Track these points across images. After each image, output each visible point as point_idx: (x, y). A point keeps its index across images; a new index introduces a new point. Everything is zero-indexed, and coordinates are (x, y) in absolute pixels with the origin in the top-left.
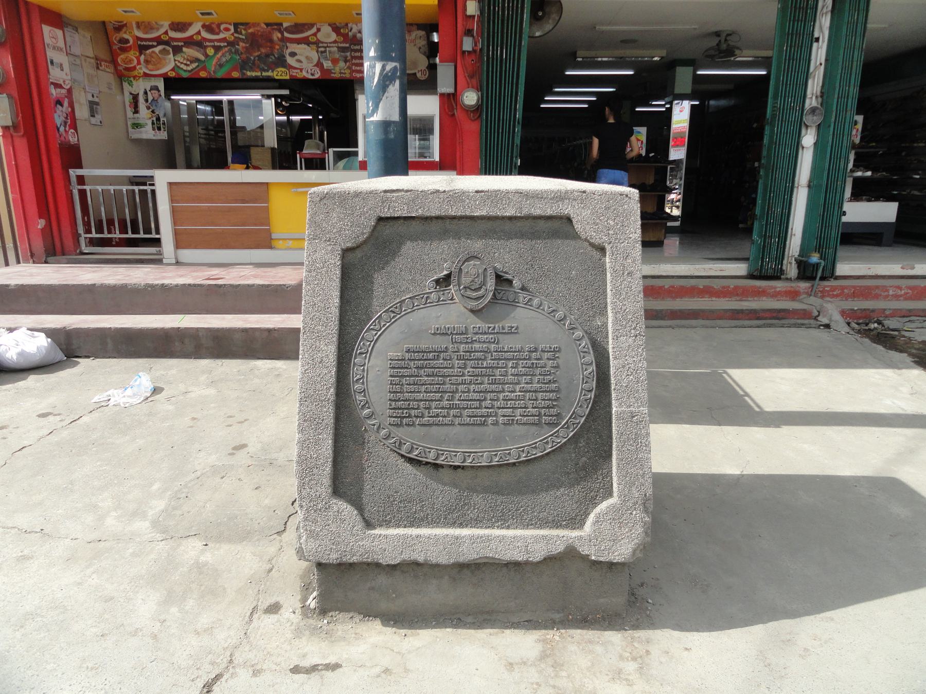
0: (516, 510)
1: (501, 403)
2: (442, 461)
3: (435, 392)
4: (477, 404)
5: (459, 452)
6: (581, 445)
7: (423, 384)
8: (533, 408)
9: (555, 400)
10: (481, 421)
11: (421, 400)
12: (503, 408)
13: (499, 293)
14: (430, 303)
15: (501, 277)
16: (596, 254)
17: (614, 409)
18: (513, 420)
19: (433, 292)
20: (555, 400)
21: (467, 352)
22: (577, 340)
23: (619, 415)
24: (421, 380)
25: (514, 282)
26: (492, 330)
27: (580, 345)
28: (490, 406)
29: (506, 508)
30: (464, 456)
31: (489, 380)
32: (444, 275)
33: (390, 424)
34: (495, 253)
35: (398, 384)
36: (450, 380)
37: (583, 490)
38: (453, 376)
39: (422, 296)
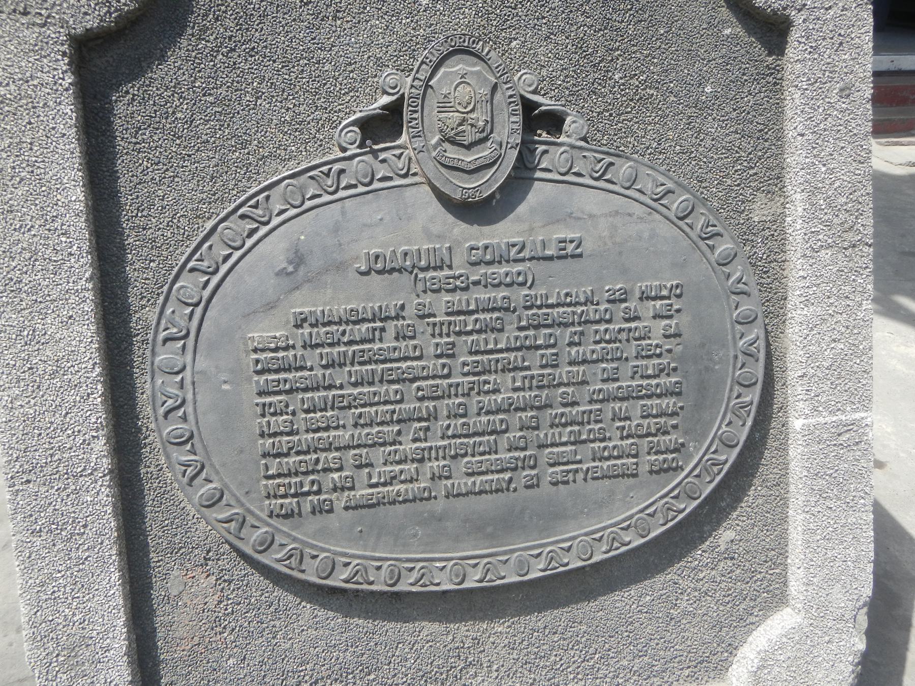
0: (582, 662)
1: (546, 435)
2: (411, 584)
3: (382, 423)
5: (451, 559)
6: (723, 504)
7: (349, 407)
8: (622, 438)
9: (674, 414)
11: (348, 447)
12: (553, 445)
14: (346, 188)
15: (537, 105)
17: (797, 424)
18: (576, 471)
20: (674, 414)
21: (459, 313)
22: (724, 265)
23: (809, 431)
24: (343, 396)
25: (569, 120)
26: (520, 252)
27: (728, 276)
28: (522, 444)
29: (561, 659)
31: (514, 380)
32: (384, 108)
33: (271, 516)
35: (281, 414)
36: (419, 389)
37: (727, 599)
38: (426, 378)
39: (325, 169)
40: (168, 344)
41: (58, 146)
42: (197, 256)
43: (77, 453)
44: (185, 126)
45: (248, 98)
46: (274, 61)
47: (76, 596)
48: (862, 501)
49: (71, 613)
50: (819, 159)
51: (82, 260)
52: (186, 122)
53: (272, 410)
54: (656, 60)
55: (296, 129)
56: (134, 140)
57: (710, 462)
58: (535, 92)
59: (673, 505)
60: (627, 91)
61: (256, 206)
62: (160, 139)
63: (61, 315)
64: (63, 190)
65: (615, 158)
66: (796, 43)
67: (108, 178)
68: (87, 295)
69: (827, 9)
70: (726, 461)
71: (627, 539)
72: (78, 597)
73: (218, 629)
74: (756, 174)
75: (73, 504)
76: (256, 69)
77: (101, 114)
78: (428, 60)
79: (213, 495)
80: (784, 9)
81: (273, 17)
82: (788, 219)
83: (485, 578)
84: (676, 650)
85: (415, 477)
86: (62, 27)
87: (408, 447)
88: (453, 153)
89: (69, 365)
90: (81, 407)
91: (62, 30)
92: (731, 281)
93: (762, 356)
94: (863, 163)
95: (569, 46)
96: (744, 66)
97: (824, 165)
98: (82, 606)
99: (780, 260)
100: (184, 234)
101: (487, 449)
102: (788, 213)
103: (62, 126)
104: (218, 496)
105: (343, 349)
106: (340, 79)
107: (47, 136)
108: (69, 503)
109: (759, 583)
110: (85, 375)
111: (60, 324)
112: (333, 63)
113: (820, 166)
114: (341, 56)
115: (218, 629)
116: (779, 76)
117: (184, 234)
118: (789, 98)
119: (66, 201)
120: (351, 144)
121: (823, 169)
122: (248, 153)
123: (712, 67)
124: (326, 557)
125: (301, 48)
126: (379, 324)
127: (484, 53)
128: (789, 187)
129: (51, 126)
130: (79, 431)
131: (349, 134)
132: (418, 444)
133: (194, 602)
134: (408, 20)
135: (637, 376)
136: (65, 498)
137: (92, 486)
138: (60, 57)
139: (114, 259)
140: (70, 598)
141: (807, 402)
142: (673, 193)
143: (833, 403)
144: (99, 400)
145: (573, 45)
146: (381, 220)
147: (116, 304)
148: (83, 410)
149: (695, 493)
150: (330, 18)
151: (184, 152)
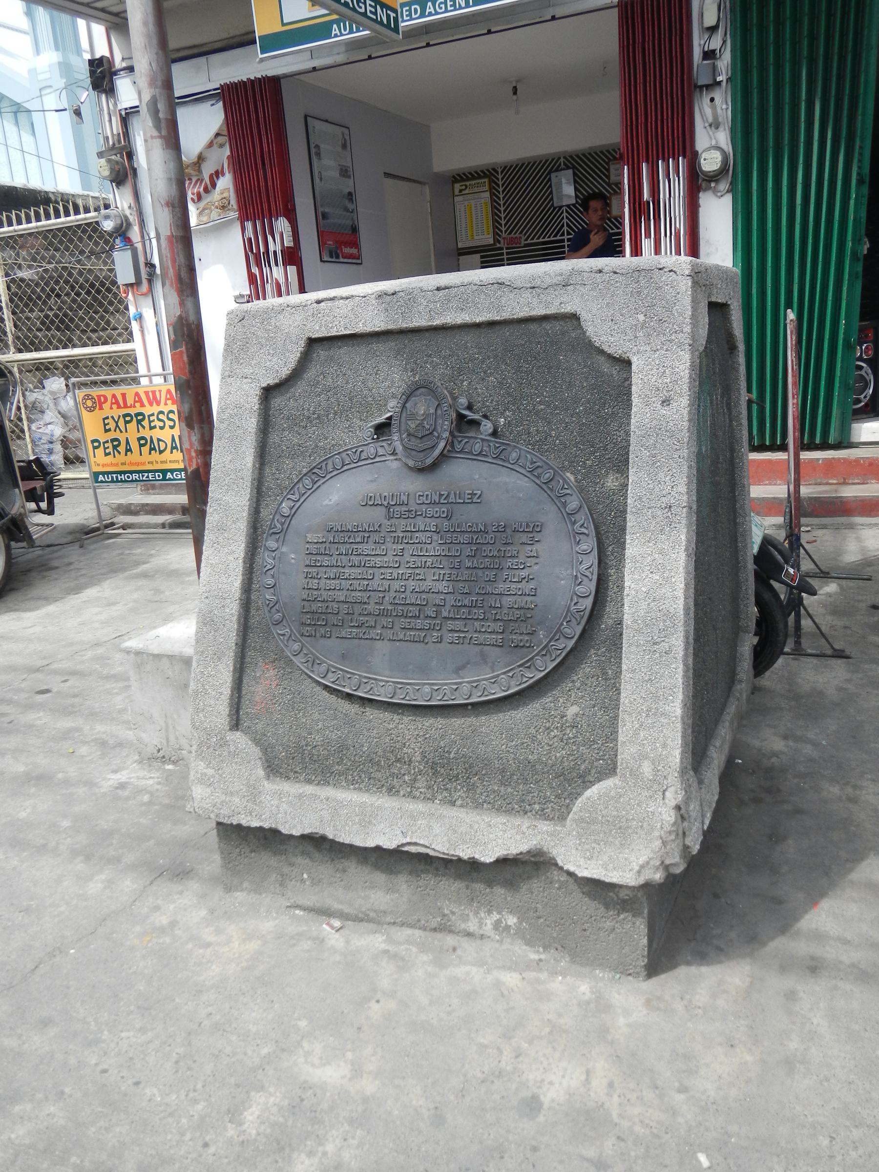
4: (414, 610)
5: (388, 682)
15: (464, 416)
30: (395, 688)
32: (387, 419)
34: (463, 381)
40: (273, 536)
42: (292, 492)
48: (671, 698)
61: (320, 469)
69: (655, 351)
73: (274, 701)
74: (609, 458)
80: (626, 353)
84: (530, 787)
88: (414, 442)
93: (595, 577)
94: (680, 450)
105: (348, 546)
109: (596, 752)
115: (274, 701)
126: (367, 535)
135: (508, 581)
142: (541, 467)
143: (649, 618)
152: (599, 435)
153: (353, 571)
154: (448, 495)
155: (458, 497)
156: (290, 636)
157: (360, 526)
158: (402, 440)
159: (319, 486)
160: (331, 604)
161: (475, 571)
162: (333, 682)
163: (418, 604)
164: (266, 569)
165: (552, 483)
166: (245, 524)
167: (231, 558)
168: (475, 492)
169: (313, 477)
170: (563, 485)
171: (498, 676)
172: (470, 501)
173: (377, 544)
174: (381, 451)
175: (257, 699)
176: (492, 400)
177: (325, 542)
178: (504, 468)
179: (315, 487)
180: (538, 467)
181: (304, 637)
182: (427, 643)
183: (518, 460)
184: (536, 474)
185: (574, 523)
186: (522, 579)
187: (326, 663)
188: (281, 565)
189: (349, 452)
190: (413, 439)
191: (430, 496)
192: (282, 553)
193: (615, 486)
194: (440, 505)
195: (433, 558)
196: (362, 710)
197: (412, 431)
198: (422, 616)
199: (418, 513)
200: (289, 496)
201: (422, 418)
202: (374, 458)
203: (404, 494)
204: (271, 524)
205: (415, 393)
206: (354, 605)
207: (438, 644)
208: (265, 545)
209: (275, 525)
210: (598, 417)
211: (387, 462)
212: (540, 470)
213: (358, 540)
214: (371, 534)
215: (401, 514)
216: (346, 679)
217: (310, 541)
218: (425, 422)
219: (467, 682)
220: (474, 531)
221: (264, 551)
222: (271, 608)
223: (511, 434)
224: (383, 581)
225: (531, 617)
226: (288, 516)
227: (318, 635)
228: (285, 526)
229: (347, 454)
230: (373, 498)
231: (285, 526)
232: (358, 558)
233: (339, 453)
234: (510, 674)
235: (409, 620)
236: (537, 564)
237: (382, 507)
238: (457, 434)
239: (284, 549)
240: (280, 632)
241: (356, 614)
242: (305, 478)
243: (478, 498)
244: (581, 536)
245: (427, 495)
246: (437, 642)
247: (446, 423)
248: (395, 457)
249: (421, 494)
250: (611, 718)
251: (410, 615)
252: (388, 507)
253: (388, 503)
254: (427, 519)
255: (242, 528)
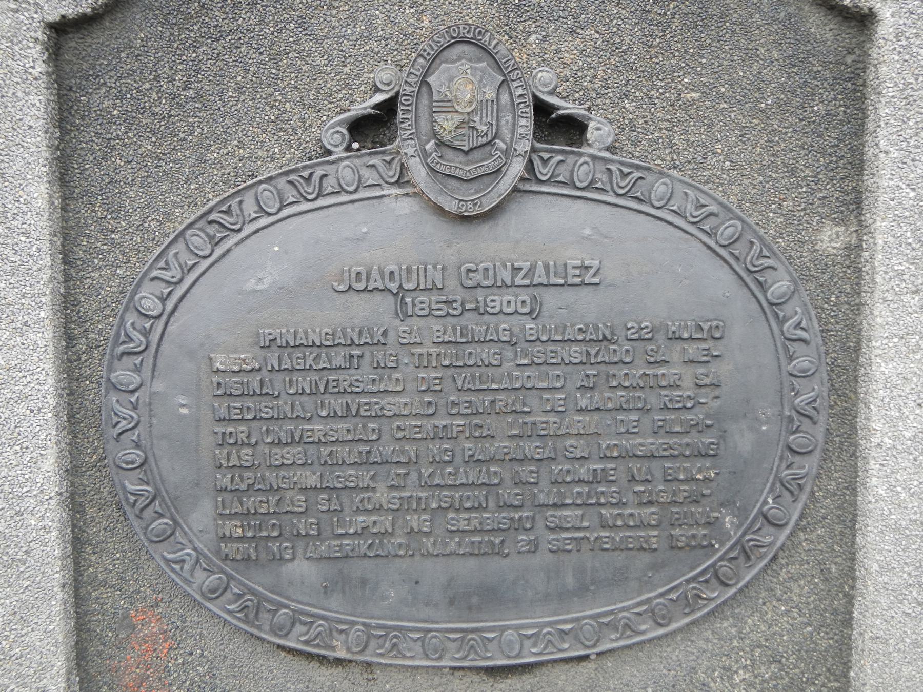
5: (430, 630)
8: (641, 504)
10: (492, 544)
13: (545, 162)
15: (552, 108)
16: (848, 35)
19: (340, 160)
25: (592, 125)
32: (377, 106)
34: (530, 34)
40: (125, 358)
41: (24, 139)
42: (162, 264)
43: (23, 472)
44: (163, 123)
45: (231, 94)
46: (261, 53)
47: (14, 627)
49: (8, 646)
50: (907, 182)
51: (41, 262)
52: (164, 117)
53: (232, 441)
54: (704, 61)
55: (281, 129)
56: (109, 136)
57: (752, 543)
58: (552, 92)
59: (702, 591)
60: (667, 95)
61: (228, 212)
62: (135, 136)
63: (16, 320)
64: (26, 186)
65: (646, 172)
66: (881, 41)
67: (78, 176)
68: (43, 300)
70: (771, 544)
71: (643, 627)
72: (16, 630)
75: (16, 526)
76: (241, 62)
77: (76, 107)
78: (426, 53)
79: (164, 531)
81: (262, 6)
82: (866, 254)
83: (466, 656)
85: (390, 531)
86: (36, 13)
87: (382, 495)
89: (21, 375)
90: (31, 422)
91: (35, 16)
92: (787, 325)
95: (599, 42)
96: (815, 69)
97: (914, 190)
98: (20, 640)
99: (852, 303)
100: (154, 239)
101: (476, 505)
102: (864, 246)
103: (29, 118)
104: (169, 532)
106: (333, 75)
107: (13, 128)
108: (12, 526)
110: (37, 387)
111: (14, 330)
112: (325, 57)
113: (908, 190)
114: (335, 49)
116: (860, 82)
117: (154, 239)
118: (870, 108)
119: (29, 198)
120: (336, 146)
121: (912, 194)
122: (227, 154)
123: (775, 69)
124: (284, 614)
125: (291, 39)
126: (356, 352)
127: (491, 47)
128: (868, 215)
129: (18, 117)
130: (27, 448)
131: (336, 136)
132: (395, 494)
133: (143, 648)
134: (412, 10)
135: (662, 431)
136: (8, 519)
137: (37, 509)
138: (31, 45)
139: (79, 263)
140: (7, 629)
141: (881, 480)
144: (50, 415)
145: (603, 41)
146: (365, 233)
147: (79, 311)
148: (32, 425)
149: (731, 579)
150: (325, 7)
151: (159, 151)
152: (803, 152)
153: (332, 426)
154: (532, 269)
155: (552, 275)
156: (197, 561)
157: (339, 334)
158: (425, 155)
159: (228, 251)
160: (288, 495)
161: (596, 416)
162: (306, 643)
163: (483, 484)
164: (118, 430)
165: (737, 245)
166: (49, 334)
167: (22, 409)
168: (587, 263)
169: (211, 230)
170: (761, 251)
171: (648, 601)
172: (577, 280)
173: (380, 370)
174: (370, 177)
175: (127, 679)
176: (594, 77)
177: (259, 370)
178: (642, 216)
179: (218, 252)
180: (711, 214)
181: (228, 562)
182: (507, 555)
183: (669, 200)
184: (706, 228)
185: (781, 322)
186: (692, 426)
187: (287, 607)
188: (154, 420)
189: (293, 177)
190: (449, 154)
191: (491, 273)
192: (153, 394)
193: (834, 248)
194: (513, 289)
195: (506, 393)
196: (365, 676)
197: (446, 137)
198: (492, 504)
199: (468, 306)
200: (155, 273)
201: (469, 110)
202: (356, 191)
203: (435, 267)
204: (118, 334)
205: (445, 53)
206: (342, 492)
207: (530, 555)
208: (109, 380)
209: (127, 335)
210: (801, 120)
211: (385, 200)
212: (713, 221)
213: (339, 361)
214: (367, 351)
215: (431, 309)
216: (335, 634)
217: (222, 367)
218: (477, 119)
219: (591, 617)
220: (591, 340)
221: (107, 392)
222: (142, 510)
223: (636, 145)
224: (403, 443)
225: (710, 495)
226: (158, 317)
227: (263, 555)
228: (155, 337)
229: (290, 182)
230: (364, 276)
231: (155, 337)
232: (342, 400)
233: (270, 179)
234: (673, 596)
235: (466, 516)
236: (717, 397)
237: (386, 293)
238: (538, 145)
239: (158, 386)
240: (170, 556)
241: (347, 510)
242: (189, 232)
243: (594, 275)
244: (796, 344)
245: (486, 269)
246: (528, 552)
247: (523, 122)
248: (405, 191)
249: (473, 267)
250: (837, 641)
251: (468, 505)
252: (400, 294)
253: (401, 286)
254: (486, 317)
255: (42, 343)
